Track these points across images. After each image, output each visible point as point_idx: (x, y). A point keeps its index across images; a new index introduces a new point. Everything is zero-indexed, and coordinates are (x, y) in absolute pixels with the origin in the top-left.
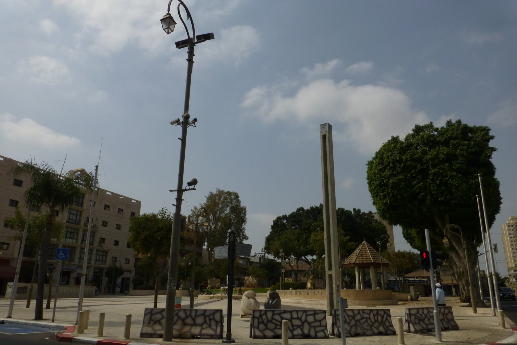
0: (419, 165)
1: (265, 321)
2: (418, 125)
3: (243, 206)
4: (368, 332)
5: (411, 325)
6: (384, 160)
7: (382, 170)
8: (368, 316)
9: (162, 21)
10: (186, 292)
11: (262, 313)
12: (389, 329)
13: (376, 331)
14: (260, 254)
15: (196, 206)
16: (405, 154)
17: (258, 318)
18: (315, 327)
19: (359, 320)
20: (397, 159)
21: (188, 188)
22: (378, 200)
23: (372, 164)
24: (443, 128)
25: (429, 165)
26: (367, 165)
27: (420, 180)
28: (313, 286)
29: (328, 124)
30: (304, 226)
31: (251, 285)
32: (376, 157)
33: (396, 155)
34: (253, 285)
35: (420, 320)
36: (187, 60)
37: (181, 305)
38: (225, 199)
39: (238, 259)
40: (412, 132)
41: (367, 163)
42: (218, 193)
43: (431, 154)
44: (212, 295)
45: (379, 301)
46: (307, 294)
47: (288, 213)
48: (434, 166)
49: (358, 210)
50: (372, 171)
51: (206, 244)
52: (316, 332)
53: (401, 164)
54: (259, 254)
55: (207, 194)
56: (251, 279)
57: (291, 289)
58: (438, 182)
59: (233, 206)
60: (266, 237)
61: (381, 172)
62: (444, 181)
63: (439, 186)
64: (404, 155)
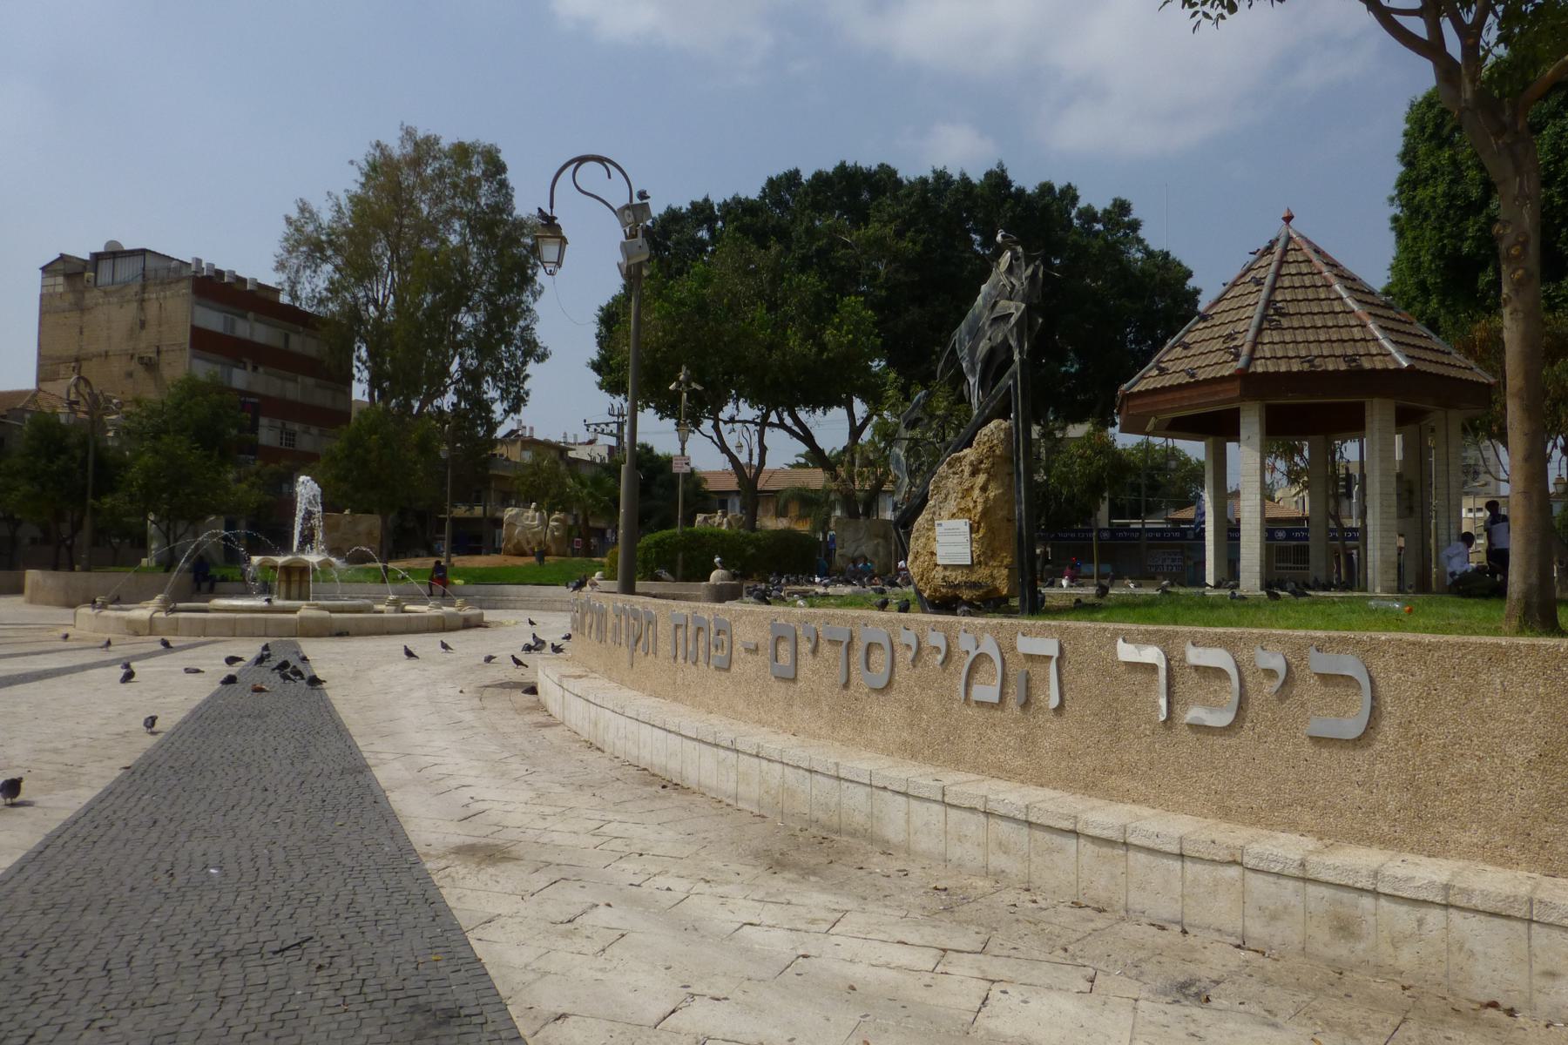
3: (524, 216)
14: (603, 426)
15: (307, 199)
30: (802, 248)
38: (440, 175)
39: (519, 444)
42: (409, 148)
46: (987, 690)
47: (719, 197)
49: (1062, 191)
54: (597, 425)
55: (362, 152)
56: (533, 518)
57: (714, 574)
60: (602, 309)
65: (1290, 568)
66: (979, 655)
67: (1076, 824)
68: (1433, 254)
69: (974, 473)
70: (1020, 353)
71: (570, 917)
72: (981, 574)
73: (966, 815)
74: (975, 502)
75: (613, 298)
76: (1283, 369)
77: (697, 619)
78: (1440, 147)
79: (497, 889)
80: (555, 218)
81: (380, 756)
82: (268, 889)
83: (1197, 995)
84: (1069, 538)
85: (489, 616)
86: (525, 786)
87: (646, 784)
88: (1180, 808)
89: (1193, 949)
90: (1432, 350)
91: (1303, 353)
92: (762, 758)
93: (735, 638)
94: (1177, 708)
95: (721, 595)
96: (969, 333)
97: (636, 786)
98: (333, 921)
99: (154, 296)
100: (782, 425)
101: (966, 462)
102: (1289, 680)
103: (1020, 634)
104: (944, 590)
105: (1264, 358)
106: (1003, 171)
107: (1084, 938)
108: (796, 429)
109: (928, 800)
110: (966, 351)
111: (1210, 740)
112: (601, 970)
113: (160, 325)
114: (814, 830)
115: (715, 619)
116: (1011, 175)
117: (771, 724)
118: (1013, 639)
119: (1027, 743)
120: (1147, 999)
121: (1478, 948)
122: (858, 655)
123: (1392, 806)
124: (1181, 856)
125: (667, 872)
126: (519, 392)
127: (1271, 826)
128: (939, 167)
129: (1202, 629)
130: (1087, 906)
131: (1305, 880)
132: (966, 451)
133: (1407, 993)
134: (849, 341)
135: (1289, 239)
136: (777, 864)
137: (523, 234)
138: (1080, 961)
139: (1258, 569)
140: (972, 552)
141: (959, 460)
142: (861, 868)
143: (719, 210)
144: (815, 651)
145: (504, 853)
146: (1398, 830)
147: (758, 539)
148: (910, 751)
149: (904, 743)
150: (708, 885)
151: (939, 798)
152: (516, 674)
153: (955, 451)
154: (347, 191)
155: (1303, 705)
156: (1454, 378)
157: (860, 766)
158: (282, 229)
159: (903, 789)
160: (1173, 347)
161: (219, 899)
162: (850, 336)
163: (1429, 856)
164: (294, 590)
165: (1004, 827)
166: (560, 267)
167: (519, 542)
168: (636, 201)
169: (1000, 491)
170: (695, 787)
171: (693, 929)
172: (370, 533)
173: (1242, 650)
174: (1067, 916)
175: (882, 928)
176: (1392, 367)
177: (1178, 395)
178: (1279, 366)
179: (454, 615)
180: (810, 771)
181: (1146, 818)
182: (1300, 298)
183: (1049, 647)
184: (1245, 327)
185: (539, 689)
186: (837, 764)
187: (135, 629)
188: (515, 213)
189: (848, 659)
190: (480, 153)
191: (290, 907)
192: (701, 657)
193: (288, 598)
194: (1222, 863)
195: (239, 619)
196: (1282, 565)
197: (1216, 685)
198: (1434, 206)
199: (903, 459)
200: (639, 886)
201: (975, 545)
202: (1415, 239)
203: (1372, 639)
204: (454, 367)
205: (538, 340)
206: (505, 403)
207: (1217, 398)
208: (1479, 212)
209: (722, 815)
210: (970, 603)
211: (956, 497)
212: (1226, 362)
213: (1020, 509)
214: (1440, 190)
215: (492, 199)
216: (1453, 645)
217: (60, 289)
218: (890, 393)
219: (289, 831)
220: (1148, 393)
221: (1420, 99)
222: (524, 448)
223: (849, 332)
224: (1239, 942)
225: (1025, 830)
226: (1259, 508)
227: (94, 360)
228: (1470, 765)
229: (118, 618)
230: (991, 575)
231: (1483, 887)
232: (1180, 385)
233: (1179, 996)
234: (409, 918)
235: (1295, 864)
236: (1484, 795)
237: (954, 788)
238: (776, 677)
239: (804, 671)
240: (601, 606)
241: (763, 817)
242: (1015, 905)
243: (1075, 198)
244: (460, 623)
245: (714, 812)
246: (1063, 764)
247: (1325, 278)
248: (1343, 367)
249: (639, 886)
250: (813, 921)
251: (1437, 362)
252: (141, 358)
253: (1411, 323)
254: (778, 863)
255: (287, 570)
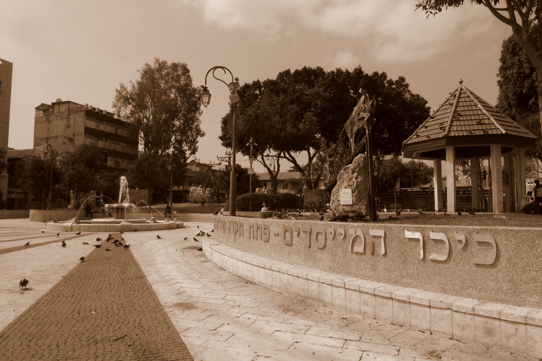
3: (196, 87)
14: (223, 158)
15: (123, 83)
38: (168, 74)
39: (195, 165)
42: (157, 65)
46: (359, 248)
47: (263, 79)
49: (381, 74)
54: (222, 158)
55: (141, 67)
56: (200, 190)
60: (223, 118)
65: (465, 204)
66: (356, 236)
67: (392, 295)
68: (513, 94)
69: (353, 173)
70: (368, 131)
71: (215, 328)
72: (356, 207)
73: (353, 292)
74: (354, 183)
75: (227, 115)
76: (461, 135)
77: (257, 224)
78: (514, 56)
79: (190, 318)
80: (207, 88)
81: (149, 272)
82: (112, 318)
83: (437, 356)
84: (386, 195)
85: (185, 224)
86: (199, 283)
87: (241, 282)
88: (429, 290)
89: (434, 340)
90: (514, 127)
91: (468, 129)
92: (281, 272)
93: (270, 231)
94: (427, 254)
95: (265, 216)
96: (350, 124)
97: (237, 282)
98: (134, 330)
99: (72, 117)
100: (285, 157)
101: (350, 169)
102: (467, 244)
103: (370, 228)
104: (343, 214)
105: (454, 131)
106: (360, 68)
107: (395, 336)
108: (290, 158)
109: (339, 287)
110: (349, 130)
111: (439, 265)
112: (226, 347)
113: (74, 127)
114: (299, 298)
115: (263, 224)
116: (363, 70)
117: (283, 261)
118: (368, 230)
119: (374, 267)
120: (418, 357)
121: (538, 339)
122: (314, 236)
123: (505, 288)
124: (430, 306)
125: (248, 313)
126: (195, 147)
127: (461, 296)
128: (338, 67)
129: (435, 226)
130: (396, 324)
131: (474, 315)
132: (350, 165)
133: (512, 355)
134: (308, 128)
135: (462, 89)
136: (287, 310)
137: (195, 93)
138: (394, 344)
139: (453, 205)
140: (353, 200)
141: (348, 168)
142: (316, 311)
143: (262, 84)
144: (298, 235)
145: (192, 306)
146: (507, 297)
147: (278, 197)
148: (332, 270)
149: (330, 267)
150: (263, 317)
151: (343, 286)
152: (195, 244)
153: (346, 165)
154: (136, 80)
155: (472, 252)
156: (522, 137)
157: (314, 275)
158: (115, 93)
159: (330, 283)
160: (422, 128)
161: (95, 321)
162: (309, 126)
163: (519, 306)
164: (120, 215)
165: (366, 297)
166: (209, 104)
167: (195, 199)
168: (235, 81)
169: (362, 179)
170: (257, 283)
171: (257, 332)
172: (145, 196)
173: (450, 233)
174: (389, 328)
175: (324, 332)
176: (499, 133)
177: (423, 144)
178: (459, 133)
179: (174, 224)
180: (297, 277)
181: (416, 293)
182: (466, 109)
183: (381, 233)
184: (447, 120)
185: (203, 249)
186: (307, 275)
187: (66, 229)
188: (193, 86)
189: (310, 238)
190: (180, 66)
191: (119, 325)
192: (259, 237)
193: (117, 218)
194: (444, 309)
195: (101, 226)
196: (462, 203)
197: (441, 246)
198: (513, 76)
199: (328, 168)
200: (239, 317)
201: (354, 197)
202: (506, 88)
203: (496, 229)
204: (173, 139)
206: (190, 151)
207: (437, 145)
208: (529, 78)
209: (267, 292)
210: (352, 218)
211: (347, 181)
212: (441, 132)
213: (369, 185)
214: (515, 71)
215: (185, 82)
216: (525, 231)
217: (41, 115)
218: (322, 145)
219: (119, 298)
220: (413, 144)
221: (507, 40)
223: (308, 125)
224: (451, 337)
225: (374, 298)
226: (453, 183)
227: (53, 139)
228: (533, 273)
229: (60, 226)
230: (360, 208)
231: (539, 317)
232: (424, 141)
233: (430, 356)
234: (160, 328)
235: (471, 309)
236: (538, 284)
237: (347, 283)
238: (285, 244)
239: (294, 243)
240: (224, 220)
241: (281, 293)
242: (371, 324)
243: (386, 77)
244: (176, 226)
245: (264, 291)
246: (387, 274)
247: (475, 103)
248: (482, 133)
249: (239, 317)
250: (300, 330)
251: (515, 131)
252: (68, 138)
253: (506, 118)
254: (287, 309)
255: (117, 209)
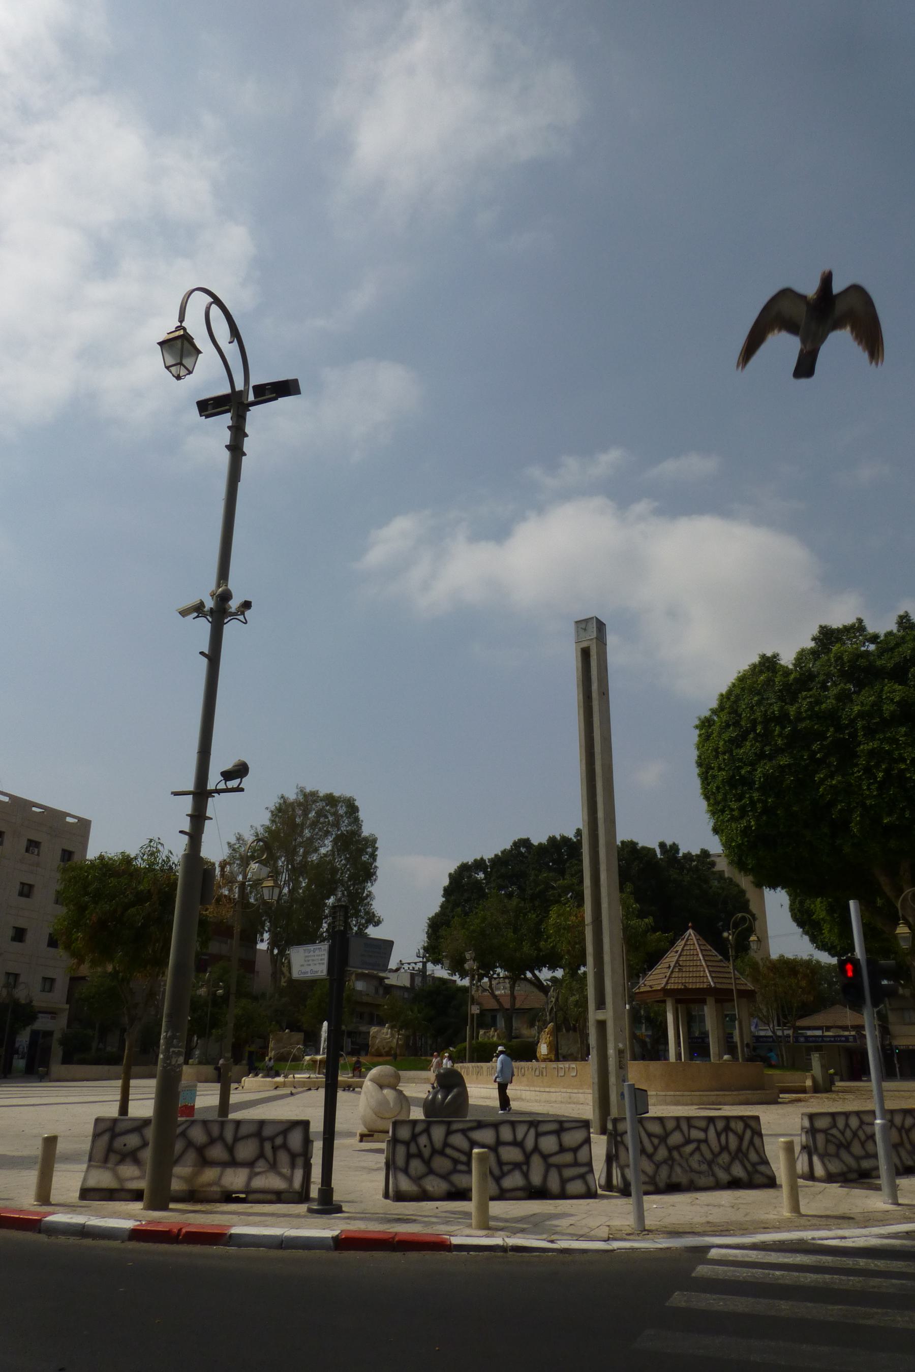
0: (832, 729)
1: (426, 1152)
2: (825, 627)
3: (368, 835)
4: (702, 1181)
5: (815, 1159)
6: (740, 715)
7: (737, 742)
8: (701, 1135)
9: (163, 346)
10: (209, 1070)
11: (419, 1128)
12: (757, 1171)
13: (723, 1176)
14: (414, 965)
15: (242, 833)
16: (794, 700)
17: (407, 1144)
18: (559, 1167)
19: (678, 1148)
20: (773, 713)
21: (222, 786)
22: (728, 821)
23: (710, 726)
24: (890, 634)
25: (856, 730)
26: (696, 727)
27: (833, 769)
28: (554, 1053)
29: (597, 618)
30: (531, 889)
31: (387, 1049)
32: (721, 708)
33: (771, 704)
34: (391, 1048)
35: (840, 1146)
36: (227, 446)
37: (194, 1106)
38: (320, 814)
39: (353, 977)
40: (812, 644)
41: (697, 722)
42: (301, 798)
43: (862, 703)
44: (280, 1079)
45: (730, 1093)
46: (537, 1073)
47: (488, 853)
48: (870, 732)
49: (670, 846)
50: (710, 745)
51: (266, 936)
52: (564, 1182)
53: (783, 728)
54: (409, 964)
55: (273, 802)
56: (387, 1034)
58: (881, 774)
59: (342, 834)
60: (429, 919)
61: (734, 748)
62: (896, 771)
63: (882, 786)
64: (792, 705)
72: (549, 1056)
77: (492, 1066)
160: (650, 975)
167: (378, 1047)
205: (375, 913)
222: (357, 979)
